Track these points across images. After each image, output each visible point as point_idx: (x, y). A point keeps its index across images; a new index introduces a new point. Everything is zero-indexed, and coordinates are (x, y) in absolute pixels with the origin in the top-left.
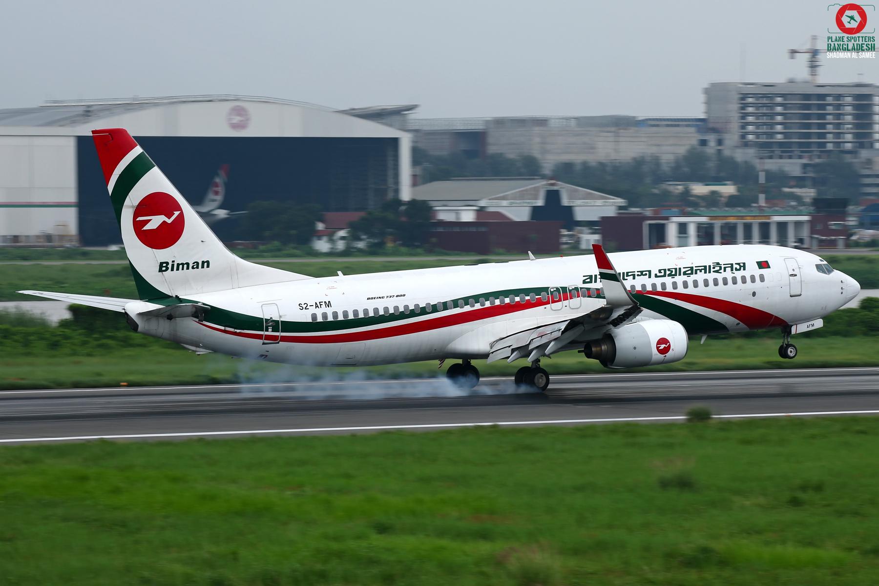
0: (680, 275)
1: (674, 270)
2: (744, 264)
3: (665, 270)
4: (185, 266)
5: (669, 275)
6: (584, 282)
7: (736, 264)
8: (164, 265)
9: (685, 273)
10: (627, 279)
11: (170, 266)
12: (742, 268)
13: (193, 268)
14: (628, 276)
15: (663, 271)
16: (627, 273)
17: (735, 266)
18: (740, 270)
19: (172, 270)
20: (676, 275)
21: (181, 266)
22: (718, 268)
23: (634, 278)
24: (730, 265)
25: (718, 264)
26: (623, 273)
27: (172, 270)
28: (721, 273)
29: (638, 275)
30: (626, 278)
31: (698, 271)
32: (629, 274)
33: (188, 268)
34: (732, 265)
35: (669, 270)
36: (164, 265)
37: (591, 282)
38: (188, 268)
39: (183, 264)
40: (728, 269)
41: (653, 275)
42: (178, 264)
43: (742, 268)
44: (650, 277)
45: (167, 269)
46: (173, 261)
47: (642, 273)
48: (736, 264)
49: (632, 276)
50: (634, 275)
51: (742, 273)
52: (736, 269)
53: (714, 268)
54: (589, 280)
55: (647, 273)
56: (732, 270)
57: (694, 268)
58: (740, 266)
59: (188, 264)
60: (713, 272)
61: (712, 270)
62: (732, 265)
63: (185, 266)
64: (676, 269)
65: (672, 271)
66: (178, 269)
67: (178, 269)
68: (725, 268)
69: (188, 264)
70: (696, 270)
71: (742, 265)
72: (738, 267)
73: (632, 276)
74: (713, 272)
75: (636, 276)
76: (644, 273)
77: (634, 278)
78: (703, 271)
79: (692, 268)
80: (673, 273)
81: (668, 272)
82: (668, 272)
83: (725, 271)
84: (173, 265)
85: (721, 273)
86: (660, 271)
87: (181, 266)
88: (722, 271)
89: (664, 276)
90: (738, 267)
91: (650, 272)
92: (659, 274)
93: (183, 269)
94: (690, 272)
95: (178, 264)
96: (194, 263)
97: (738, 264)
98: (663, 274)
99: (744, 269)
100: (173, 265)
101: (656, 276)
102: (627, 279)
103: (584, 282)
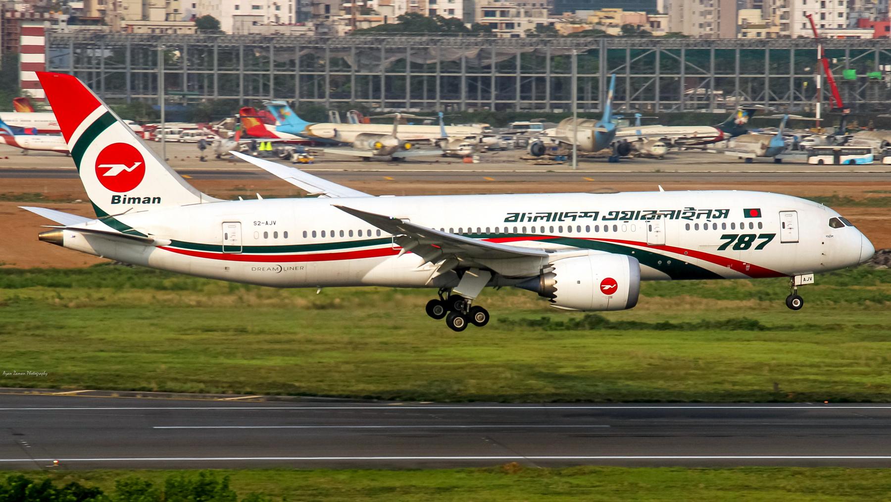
0: (636, 218)
1: (629, 214)
2: (728, 211)
3: (618, 213)
4: (137, 200)
5: (621, 219)
6: (507, 220)
7: (716, 210)
8: (117, 198)
9: (643, 218)
10: (564, 221)
11: (122, 199)
12: (723, 215)
13: (144, 202)
14: (566, 216)
15: (614, 214)
16: (567, 213)
17: (713, 213)
18: (719, 217)
19: (124, 202)
20: (631, 218)
21: (132, 200)
22: (690, 214)
23: (574, 220)
24: (707, 212)
25: (692, 209)
26: (562, 214)
27: (124, 202)
28: (692, 220)
29: (580, 216)
30: (563, 218)
31: (662, 216)
32: (569, 215)
33: (139, 202)
34: (710, 211)
35: (623, 213)
36: (117, 198)
37: (516, 220)
38: (139, 202)
39: (134, 199)
40: (703, 217)
41: (600, 217)
42: (130, 199)
43: (723, 215)
44: (595, 219)
45: (119, 201)
46: (125, 196)
47: (586, 214)
48: (716, 210)
49: (572, 218)
50: (574, 218)
51: (722, 220)
52: (714, 217)
53: (684, 213)
54: (513, 218)
55: (594, 215)
56: (709, 217)
57: (657, 213)
58: (721, 213)
59: (139, 199)
60: (682, 217)
61: (681, 215)
62: (710, 211)
63: (137, 200)
64: (633, 213)
65: (627, 215)
66: (129, 202)
67: (129, 202)
68: (699, 215)
69: (139, 199)
70: (659, 217)
71: (724, 212)
72: (717, 214)
73: (572, 218)
74: (682, 217)
75: (577, 217)
76: (589, 215)
77: (574, 220)
78: (669, 216)
79: (655, 212)
80: (628, 217)
81: (621, 215)
82: (621, 215)
83: (698, 217)
84: (125, 199)
85: (692, 220)
86: (610, 213)
87: (132, 200)
88: (694, 218)
89: (615, 219)
90: (717, 214)
91: (597, 213)
92: (608, 217)
93: (134, 202)
94: (650, 216)
95: (130, 199)
96: (145, 198)
97: (720, 211)
98: (613, 217)
99: (725, 217)
100: (125, 199)
101: (604, 218)
102: (564, 221)
103: (507, 220)
